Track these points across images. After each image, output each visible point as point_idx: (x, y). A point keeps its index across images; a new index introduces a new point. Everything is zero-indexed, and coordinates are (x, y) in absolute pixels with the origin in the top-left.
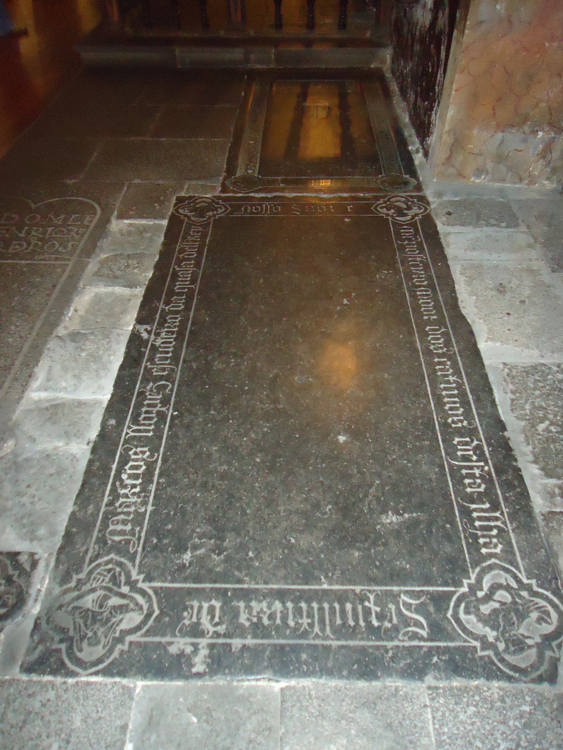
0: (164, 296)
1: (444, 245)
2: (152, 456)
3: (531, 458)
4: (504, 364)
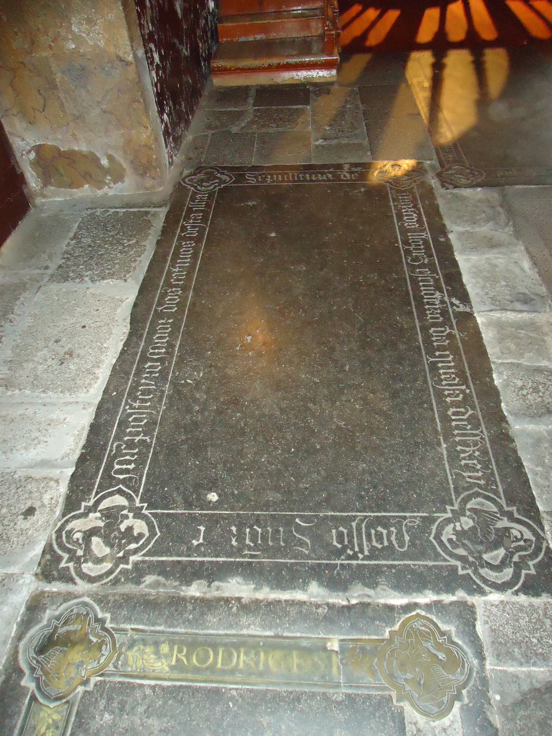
0: (460, 345)
1: (87, 428)
2: (402, 224)
3: (153, 228)
4: (125, 281)
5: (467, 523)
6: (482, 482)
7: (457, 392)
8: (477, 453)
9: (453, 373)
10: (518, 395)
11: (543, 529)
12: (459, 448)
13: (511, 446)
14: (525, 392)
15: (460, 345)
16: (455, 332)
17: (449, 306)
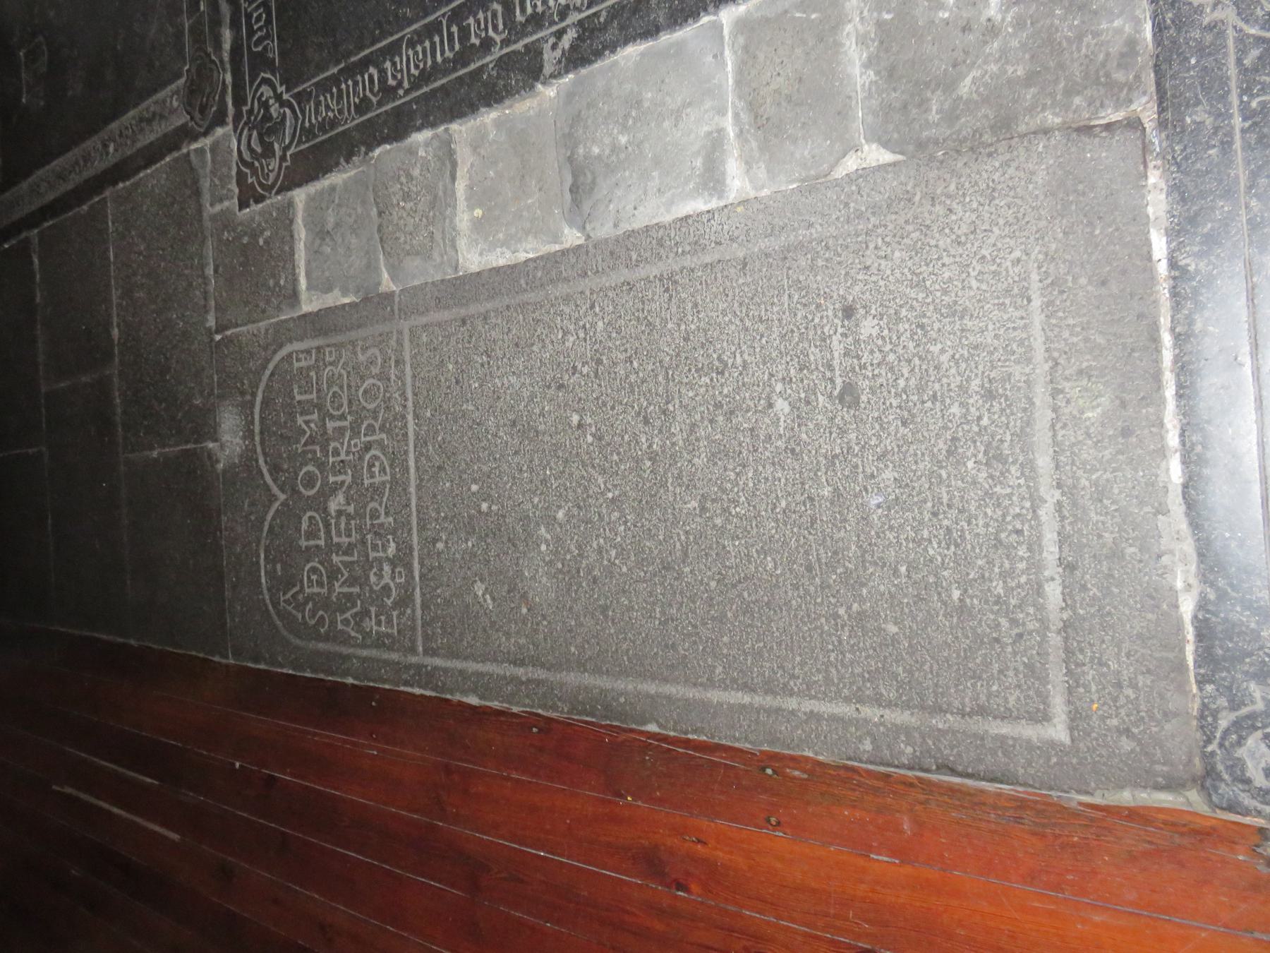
0: (473, 67)
5: (274, 110)
6: (307, 124)
7: (399, 76)
8: (330, 114)
9: (425, 63)
10: (399, 169)
11: (278, 193)
12: (334, 90)
13: (342, 160)
14: (403, 179)
15: (473, 67)
16: (497, 53)
17: (555, 28)
